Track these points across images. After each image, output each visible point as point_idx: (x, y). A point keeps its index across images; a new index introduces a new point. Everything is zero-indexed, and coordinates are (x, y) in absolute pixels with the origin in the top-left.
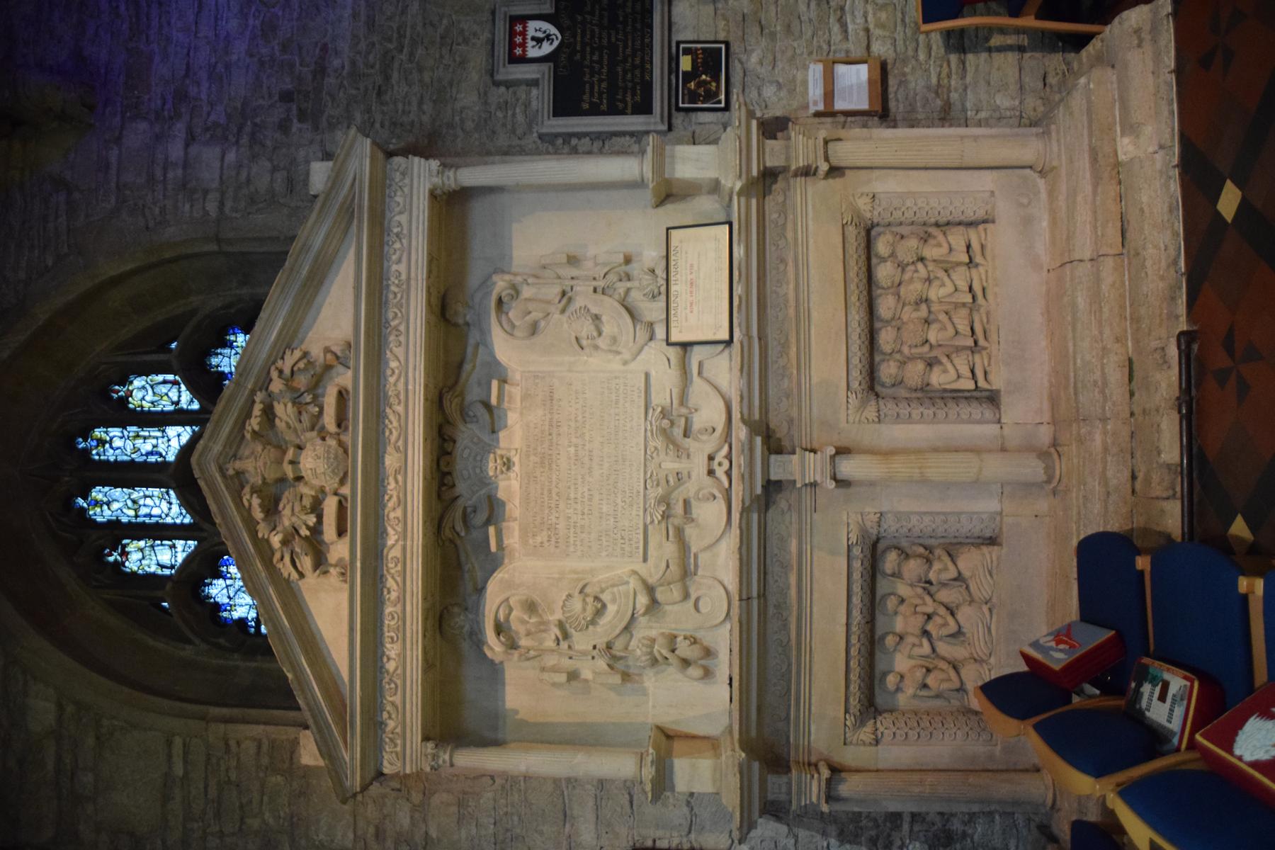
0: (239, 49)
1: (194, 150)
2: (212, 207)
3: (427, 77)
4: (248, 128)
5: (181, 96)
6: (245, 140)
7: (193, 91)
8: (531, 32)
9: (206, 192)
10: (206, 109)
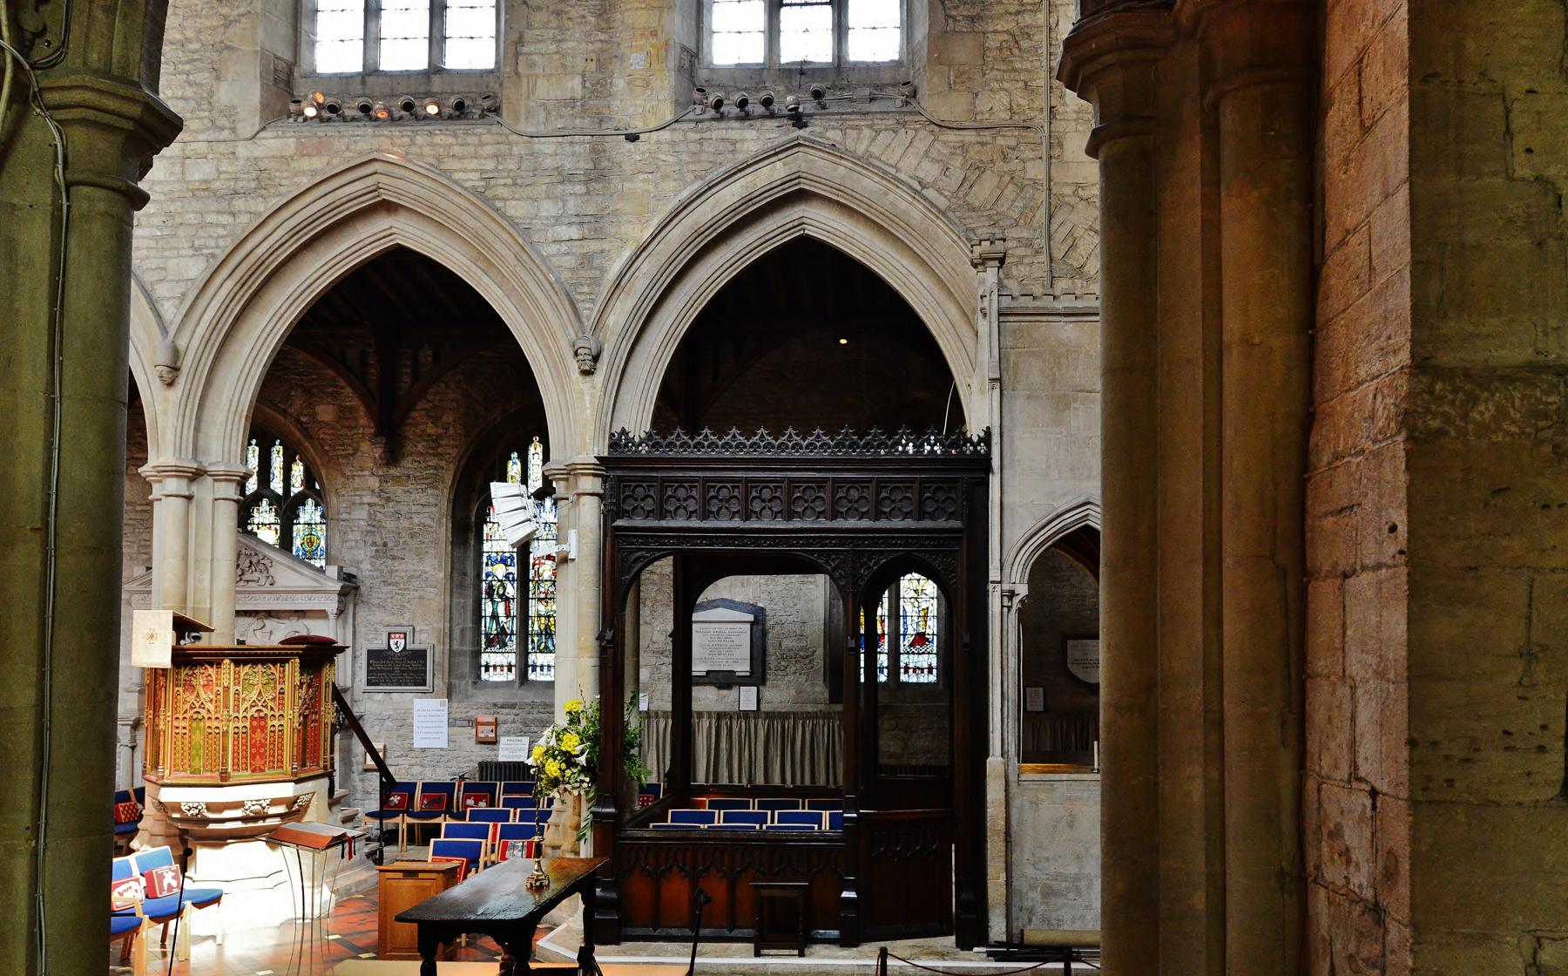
0: (405, 523)
1: (367, 507)
2: (344, 516)
3: (389, 600)
4: (373, 529)
5: (388, 499)
6: (369, 528)
7: (391, 504)
8: (399, 641)
9: (349, 513)
10: (383, 511)
